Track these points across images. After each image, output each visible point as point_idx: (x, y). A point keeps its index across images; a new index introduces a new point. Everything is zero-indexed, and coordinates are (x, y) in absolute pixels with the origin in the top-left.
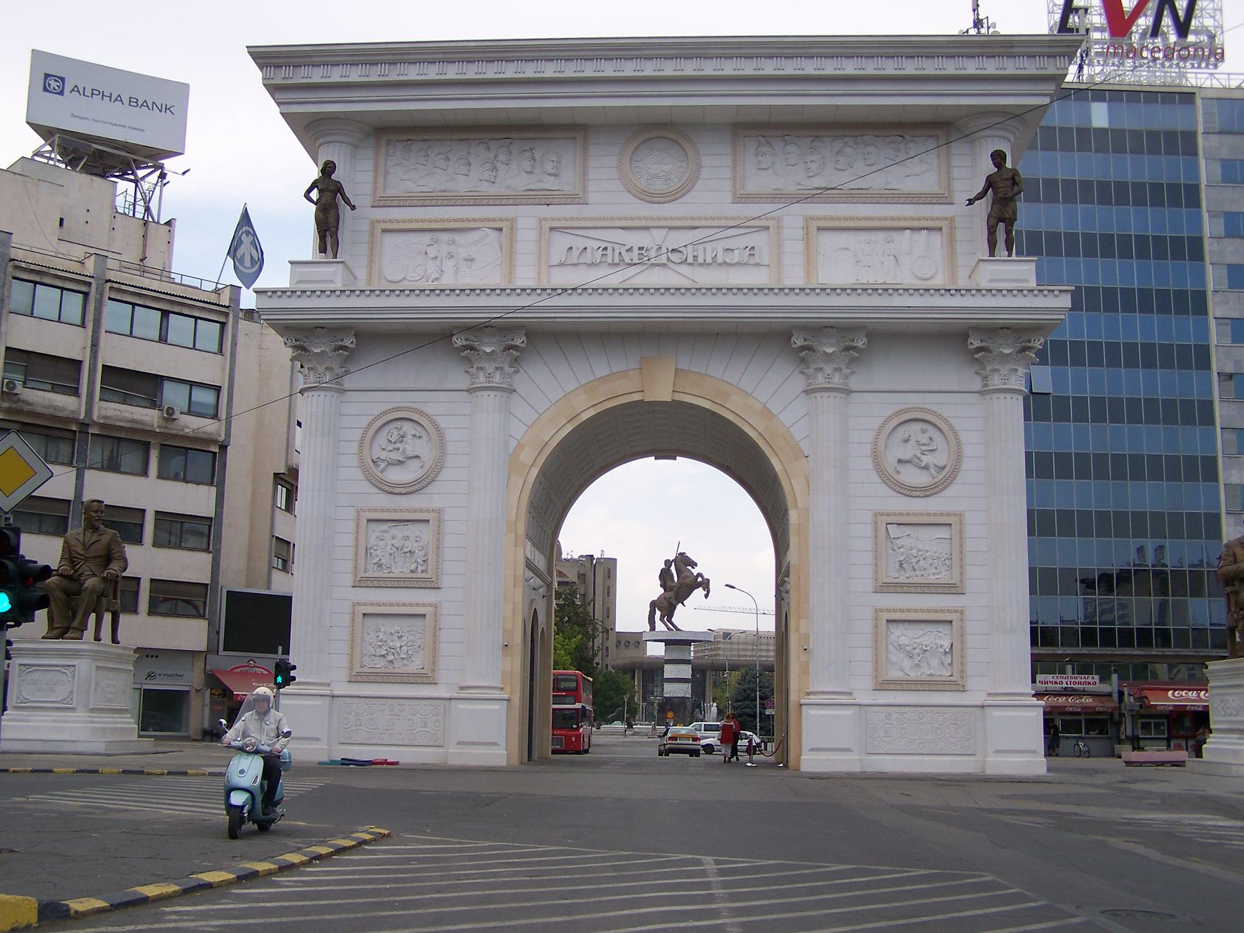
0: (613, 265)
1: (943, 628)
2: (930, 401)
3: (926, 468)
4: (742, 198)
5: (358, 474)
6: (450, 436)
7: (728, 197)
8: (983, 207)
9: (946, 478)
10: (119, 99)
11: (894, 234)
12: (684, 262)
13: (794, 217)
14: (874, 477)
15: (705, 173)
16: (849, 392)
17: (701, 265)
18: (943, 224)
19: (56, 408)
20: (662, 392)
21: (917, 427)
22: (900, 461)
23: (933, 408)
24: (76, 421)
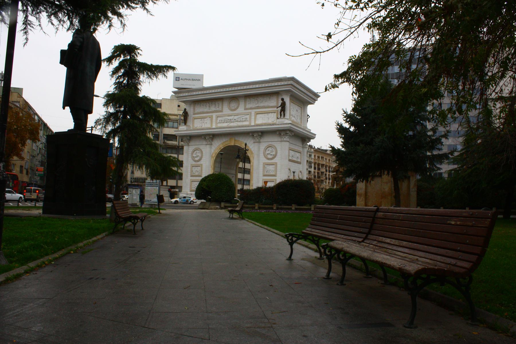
0: (226, 122)
2: (273, 143)
3: (271, 155)
4: (246, 109)
5: (191, 159)
6: (204, 152)
7: (243, 109)
8: (280, 108)
9: (275, 156)
10: (190, 80)
11: (269, 114)
13: (253, 112)
15: (240, 105)
18: (276, 111)
19: (173, 144)
20: (232, 144)
21: (270, 148)
22: (267, 154)
23: (274, 145)
24: (177, 146)
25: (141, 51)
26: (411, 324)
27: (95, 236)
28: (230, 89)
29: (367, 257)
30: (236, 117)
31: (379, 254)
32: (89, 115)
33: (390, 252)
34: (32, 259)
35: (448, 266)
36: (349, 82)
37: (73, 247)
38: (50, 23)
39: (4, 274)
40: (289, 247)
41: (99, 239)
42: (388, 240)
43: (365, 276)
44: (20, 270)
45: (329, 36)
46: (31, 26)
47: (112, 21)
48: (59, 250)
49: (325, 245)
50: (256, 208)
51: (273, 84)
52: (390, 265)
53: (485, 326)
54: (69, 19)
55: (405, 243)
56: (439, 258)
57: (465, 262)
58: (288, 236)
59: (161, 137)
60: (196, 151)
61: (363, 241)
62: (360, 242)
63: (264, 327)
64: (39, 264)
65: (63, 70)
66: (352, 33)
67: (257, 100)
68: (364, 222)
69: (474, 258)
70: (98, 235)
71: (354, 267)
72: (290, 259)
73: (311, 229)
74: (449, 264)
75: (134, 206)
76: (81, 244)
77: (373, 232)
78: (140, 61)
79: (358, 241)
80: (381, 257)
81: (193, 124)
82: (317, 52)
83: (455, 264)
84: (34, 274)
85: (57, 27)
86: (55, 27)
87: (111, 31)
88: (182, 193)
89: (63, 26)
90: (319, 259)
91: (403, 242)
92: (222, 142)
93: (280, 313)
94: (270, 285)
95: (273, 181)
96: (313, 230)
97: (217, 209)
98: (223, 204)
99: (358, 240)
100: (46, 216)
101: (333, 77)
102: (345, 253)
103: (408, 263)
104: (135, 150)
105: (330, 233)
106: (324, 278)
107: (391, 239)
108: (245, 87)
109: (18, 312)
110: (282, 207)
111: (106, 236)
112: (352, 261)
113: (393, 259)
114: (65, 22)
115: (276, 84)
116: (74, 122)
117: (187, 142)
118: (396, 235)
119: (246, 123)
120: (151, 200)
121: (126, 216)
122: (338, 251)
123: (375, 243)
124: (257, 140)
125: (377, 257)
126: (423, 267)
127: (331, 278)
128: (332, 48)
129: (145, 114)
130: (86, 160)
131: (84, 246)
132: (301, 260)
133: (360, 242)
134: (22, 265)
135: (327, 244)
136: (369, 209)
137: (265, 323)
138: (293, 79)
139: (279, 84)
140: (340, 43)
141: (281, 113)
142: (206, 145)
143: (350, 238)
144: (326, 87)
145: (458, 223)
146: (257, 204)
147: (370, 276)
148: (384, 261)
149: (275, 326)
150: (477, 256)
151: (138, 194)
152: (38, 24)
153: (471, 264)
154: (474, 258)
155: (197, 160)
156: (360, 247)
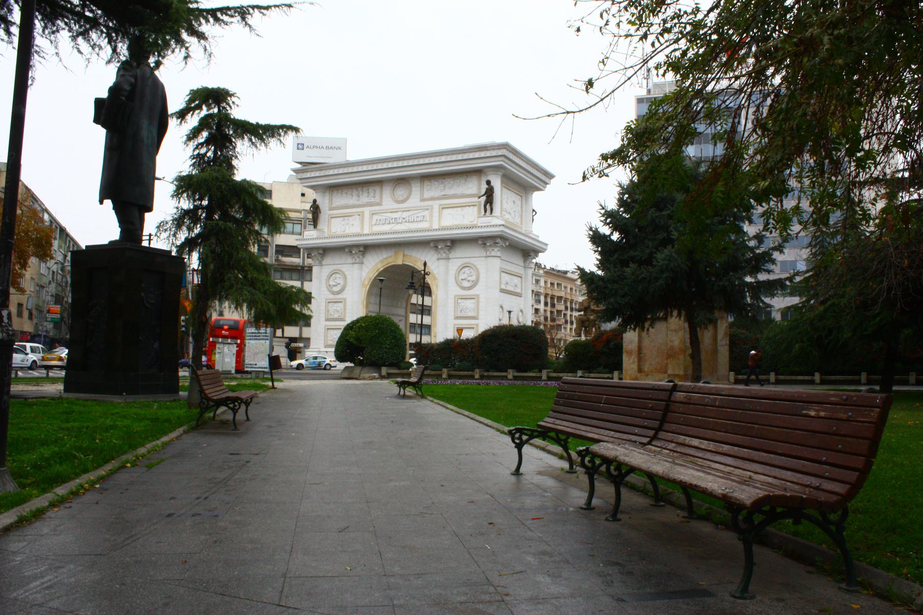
1: (471, 330)
2: (472, 261)
3: (469, 281)
4: (423, 200)
5: (326, 289)
6: (348, 277)
8: (484, 198)
9: (475, 284)
11: (464, 208)
12: (406, 222)
13: (436, 204)
14: (456, 285)
15: (413, 193)
16: (449, 259)
17: (411, 222)
19: (293, 262)
20: (400, 262)
21: (466, 269)
22: (462, 280)
24: (300, 266)
25: (239, 98)
26: (744, 592)
27: (165, 433)
28: (395, 164)
29: (663, 473)
30: (405, 215)
31: (684, 468)
32: (147, 215)
33: (699, 463)
34: (61, 480)
35: (807, 489)
36: (624, 164)
37: (130, 456)
38: (76, 50)
39: (15, 510)
40: (516, 450)
41: (173, 440)
42: (695, 442)
43: (654, 503)
44: (40, 502)
45: (590, 84)
46: (40, 56)
47: (190, 49)
48: (106, 462)
49: (584, 450)
50: (444, 376)
51: (471, 155)
52: (706, 488)
53: (871, 593)
54: (109, 42)
55: (726, 448)
56: (788, 475)
57: (836, 483)
58: (513, 432)
59: (272, 251)
60: (334, 275)
61: (649, 443)
62: (644, 444)
63: (488, 602)
64: (74, 489)
65: (101, 132)
66: (629, 79)
67: (442, 183)
68: (651, 408)
69: (853, 476)
70: (171, 432)
71: (633, 488)
72: (517, 472)
73: (554, 420)
74: (807, 486)
75: (227, 376)
76: (142, 451)
77: (667, 426)
78: (236, 118)
79: (641, 443)
80: (688, 474)
81: (328, 227)
82: (568, 113)
83: (818, 486)
84: (66, 508)
85: (88, 56)
86: (85, 58)
87: (187, 66)
88: (309, 350)
89: (98, 55)
90: (568, 472)
91: (724, 445)
92: (381, 259)
93: (515, 575)
94: (490, 522)
95: (473, 328)
96: (558, 422)
97: (374, 378)
98: (384, 371)
99: (640, 441)
100: (71, 396)
101: (597, 156)
102: (620, 465)
103: (739, 485)
104: (230, 275)
105: (588, 428)
106: (582, 508)
107: (701, 441)
108: (421, 161)
109: (50, 580)
110: (491, 374)
111: (185, 432)
112: (632, 478)
113: (710, 478)
114: (102, 49)
115: (477, 155)
116: (120, 227)
117: (318, 259)
118: (709, 434)
119: (424, 225)
120: (256, 365)
121: (219, 397)
122: (607, 461)
123: (671, 446)
124: (444, 255)
125: (681, 474)
126: (766, 493)
127: (594, 508)
128: (595, 105)
129: (247, 211)
130: (143, 294)
131: (149, 452)
132: (537, 474)
133: (644, 444)
134: (44, 491)
135: (587, 449)
136: (659, 386)
137: (490, 594)
138: (506, 146)
139: (483, 154)
140: (607, 96)
141: (485, 206)
142: (353, 264)
143: (625, 436)
144: (584, 173)
145: (822, 414)
146: (445, 370)
147: (662, 503)
148: (695, 482)
149: (509, 599)
150: (858, 473)
151: (234, 354)
152: (54, 53)
153: (848, 486)
154: (853, 476)
155: (338, 291)
156: (649, 455)
